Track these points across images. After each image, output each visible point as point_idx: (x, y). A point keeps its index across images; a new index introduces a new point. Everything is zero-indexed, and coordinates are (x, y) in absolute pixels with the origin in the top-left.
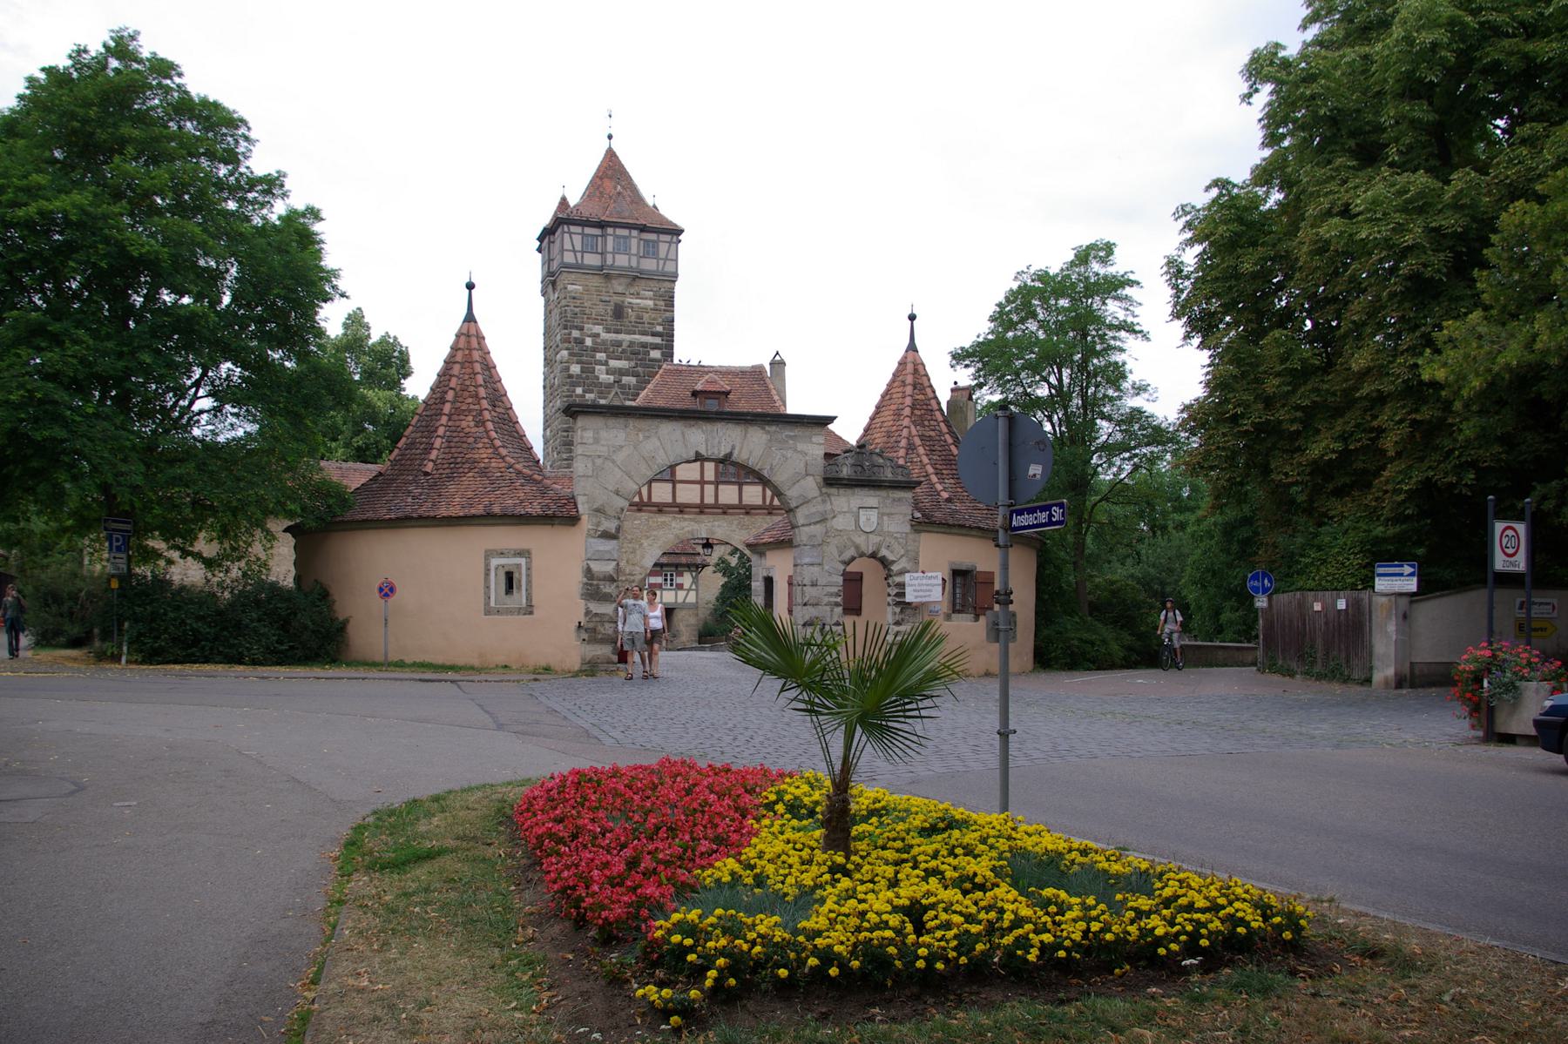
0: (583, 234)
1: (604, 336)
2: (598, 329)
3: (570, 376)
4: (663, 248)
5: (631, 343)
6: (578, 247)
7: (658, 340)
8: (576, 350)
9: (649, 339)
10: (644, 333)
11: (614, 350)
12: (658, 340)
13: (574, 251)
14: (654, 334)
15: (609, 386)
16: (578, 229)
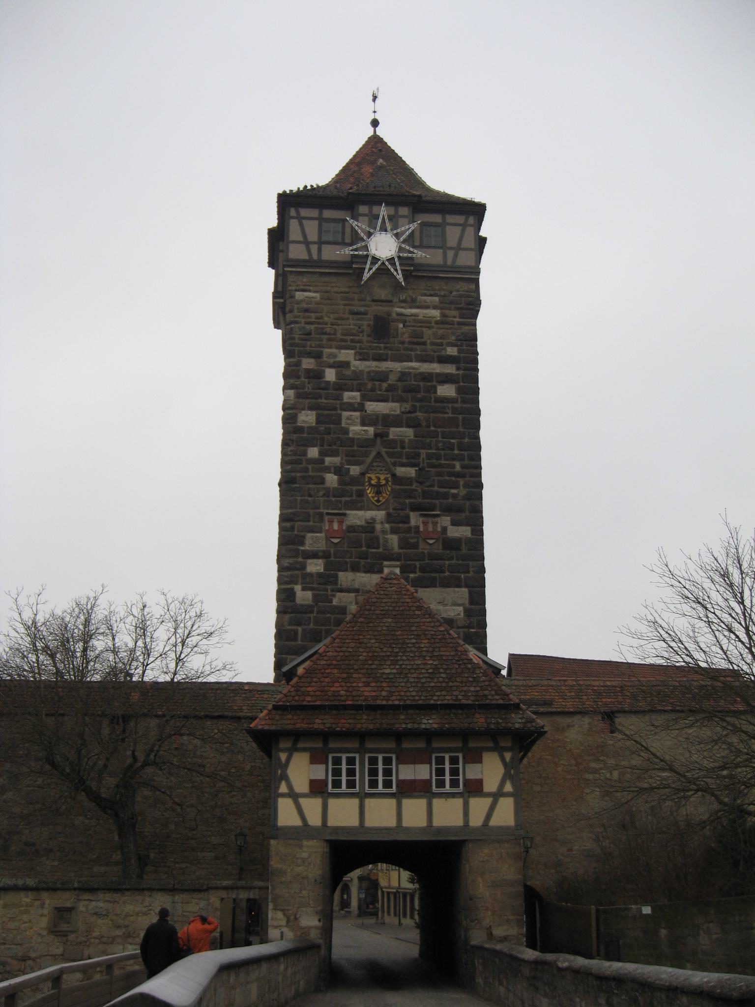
0: (321, 220)
1: (357, 365)
2: (346, 355)
3: (300, 430)
4: (452, 235)
5: (404, 376)
6: (313, 236)
7: (450, 369)
8: (309, 388)
9: (436, 368)
10: (424, 359)
11: (374, 386)
12: (450, 369)
13: (307, 243)
14: (443, 360)
15: (366, 444)
16: (314, 213)
